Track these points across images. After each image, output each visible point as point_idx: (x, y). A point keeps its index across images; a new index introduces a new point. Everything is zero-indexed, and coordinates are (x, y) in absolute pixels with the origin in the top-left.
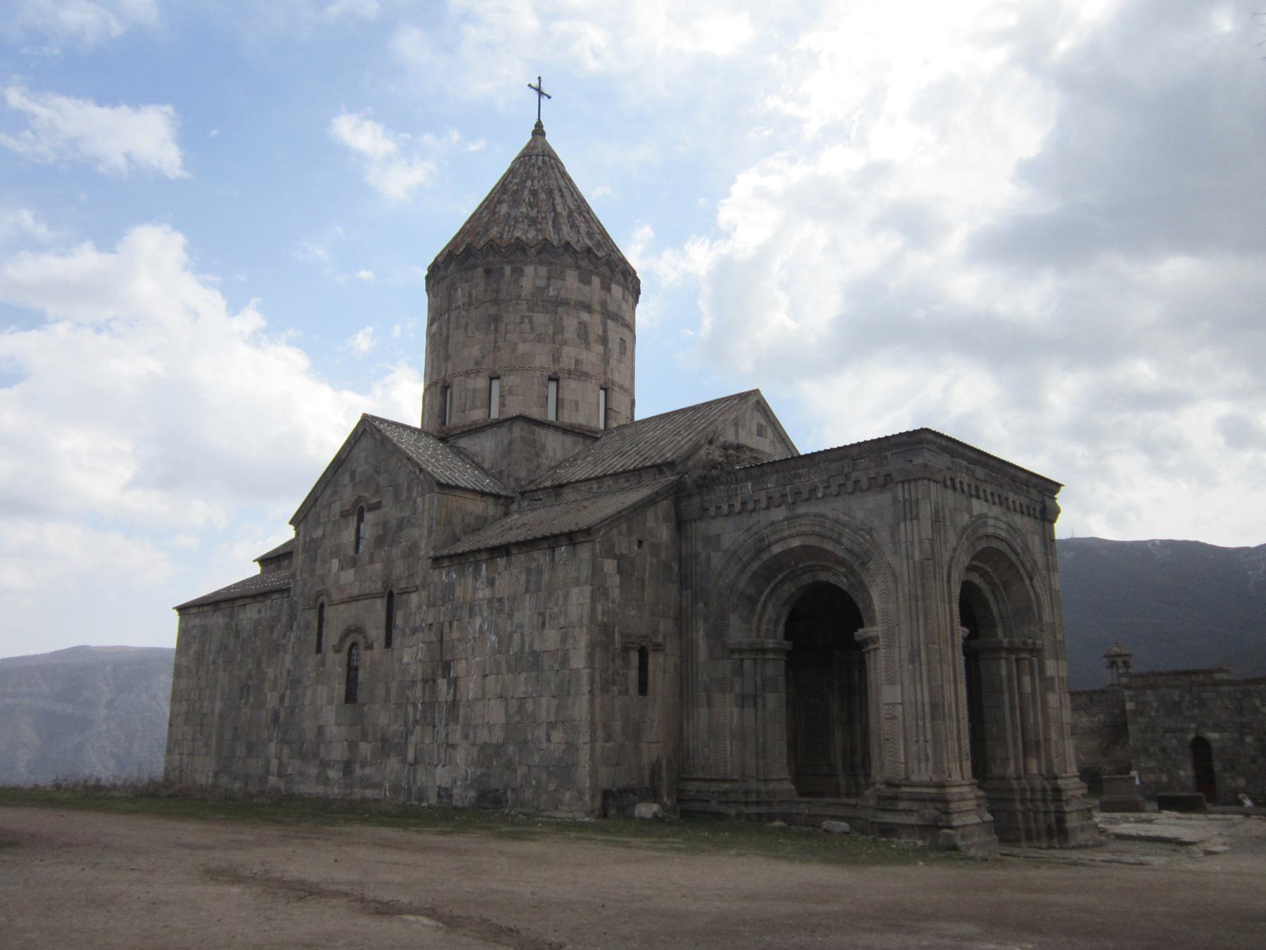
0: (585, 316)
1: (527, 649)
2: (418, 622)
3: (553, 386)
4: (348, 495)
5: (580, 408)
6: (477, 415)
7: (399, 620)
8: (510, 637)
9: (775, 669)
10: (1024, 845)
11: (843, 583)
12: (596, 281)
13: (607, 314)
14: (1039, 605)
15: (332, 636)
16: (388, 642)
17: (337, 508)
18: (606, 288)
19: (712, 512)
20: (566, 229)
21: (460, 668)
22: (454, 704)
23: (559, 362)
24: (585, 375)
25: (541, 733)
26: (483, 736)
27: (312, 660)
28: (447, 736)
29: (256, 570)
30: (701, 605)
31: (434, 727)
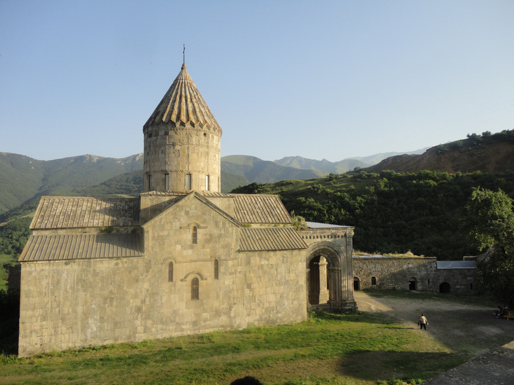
2: (233, 271)
7: (222, 269)
8: (277, 276)
17: (177, 224)
21: (255, 285)
26: (267, 305)
27: (166, 286)
28: (250, 306)
31: (244, 304)
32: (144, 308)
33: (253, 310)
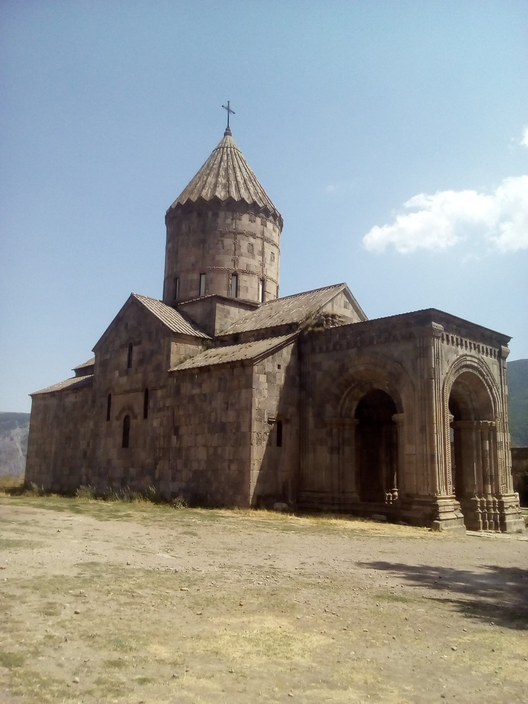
0: (252, 240)
1: (219, 421)
2: (161, 406)
3: (235, 278)
4: (124, 336)
5: (249, 291)
6: (193, 293)
7: (151, 404)
9: (349, 433)
10: (481, 530)
11: (387, 389)
12: (258, 220)
13: (264, 239)
14: (495, 403)
15: (115, 411)
16: (146, 416)
17: (118, 343)
18: (264, 225)
19: (317, 350)
20: (243, 191)
21: (183, 430)
22: (180, 449)
23: (238, 266)
24: (253, 273)
25: (226, 465)
26: (195, 466)
27: (104, 424)
29: (74, 374)
30: (311, 399)
31: (169, 460)
32: (88, 453)
33: (180, 471)
